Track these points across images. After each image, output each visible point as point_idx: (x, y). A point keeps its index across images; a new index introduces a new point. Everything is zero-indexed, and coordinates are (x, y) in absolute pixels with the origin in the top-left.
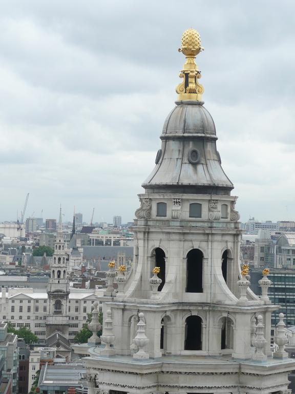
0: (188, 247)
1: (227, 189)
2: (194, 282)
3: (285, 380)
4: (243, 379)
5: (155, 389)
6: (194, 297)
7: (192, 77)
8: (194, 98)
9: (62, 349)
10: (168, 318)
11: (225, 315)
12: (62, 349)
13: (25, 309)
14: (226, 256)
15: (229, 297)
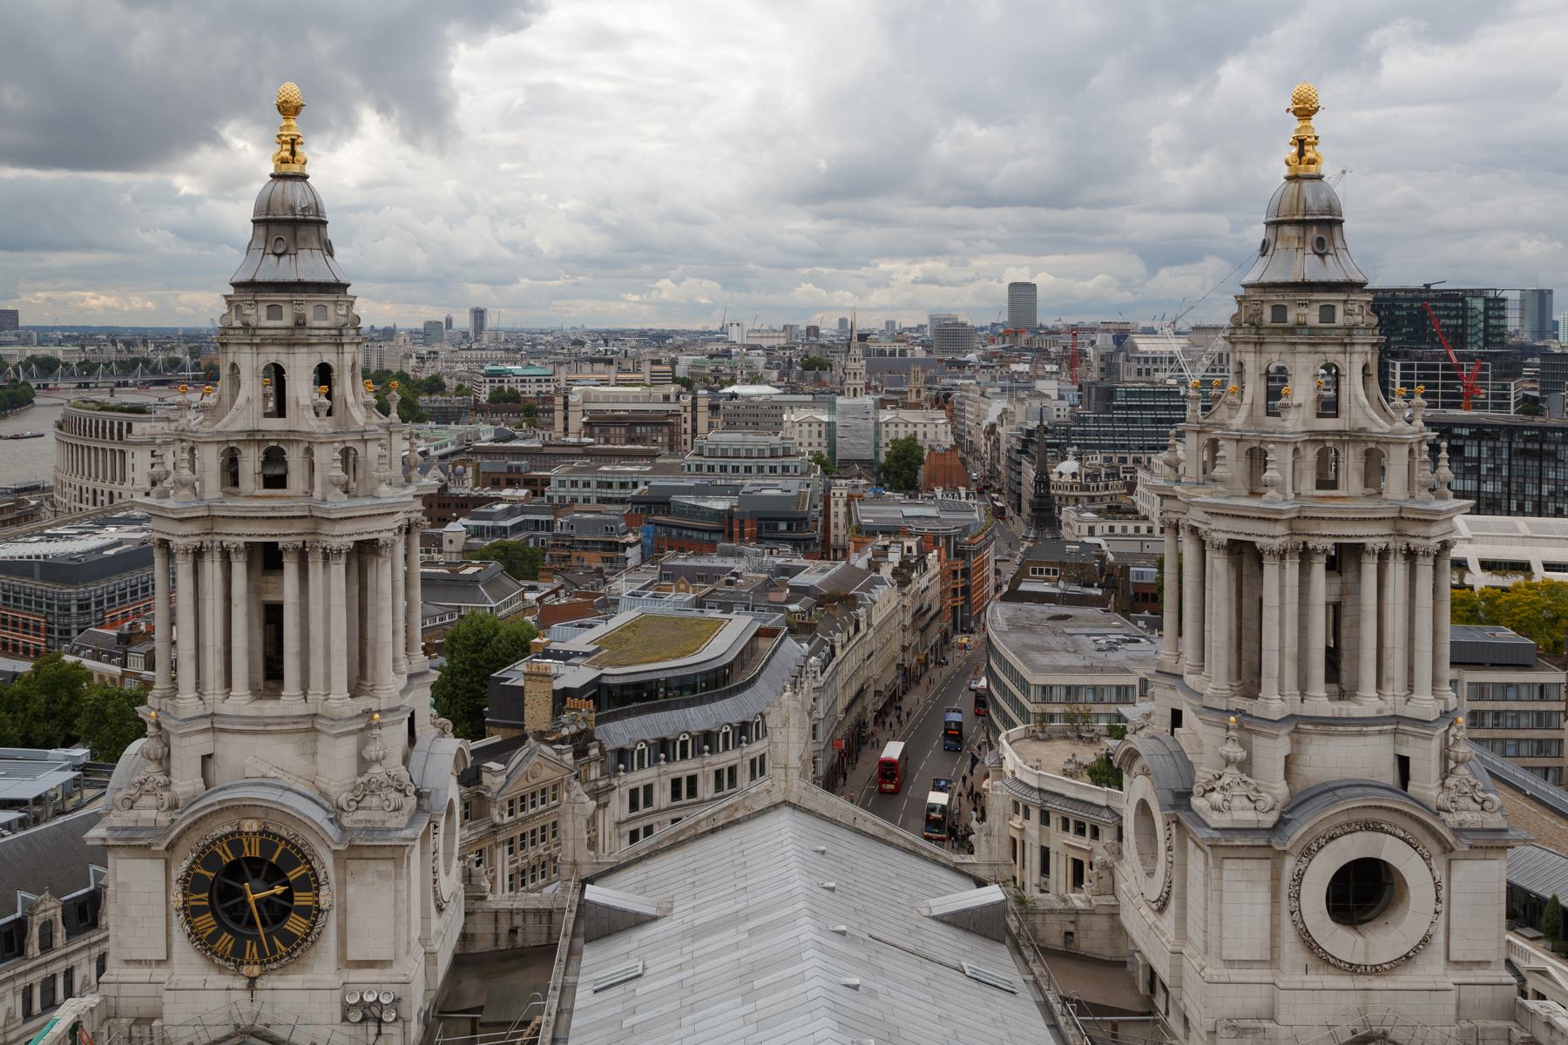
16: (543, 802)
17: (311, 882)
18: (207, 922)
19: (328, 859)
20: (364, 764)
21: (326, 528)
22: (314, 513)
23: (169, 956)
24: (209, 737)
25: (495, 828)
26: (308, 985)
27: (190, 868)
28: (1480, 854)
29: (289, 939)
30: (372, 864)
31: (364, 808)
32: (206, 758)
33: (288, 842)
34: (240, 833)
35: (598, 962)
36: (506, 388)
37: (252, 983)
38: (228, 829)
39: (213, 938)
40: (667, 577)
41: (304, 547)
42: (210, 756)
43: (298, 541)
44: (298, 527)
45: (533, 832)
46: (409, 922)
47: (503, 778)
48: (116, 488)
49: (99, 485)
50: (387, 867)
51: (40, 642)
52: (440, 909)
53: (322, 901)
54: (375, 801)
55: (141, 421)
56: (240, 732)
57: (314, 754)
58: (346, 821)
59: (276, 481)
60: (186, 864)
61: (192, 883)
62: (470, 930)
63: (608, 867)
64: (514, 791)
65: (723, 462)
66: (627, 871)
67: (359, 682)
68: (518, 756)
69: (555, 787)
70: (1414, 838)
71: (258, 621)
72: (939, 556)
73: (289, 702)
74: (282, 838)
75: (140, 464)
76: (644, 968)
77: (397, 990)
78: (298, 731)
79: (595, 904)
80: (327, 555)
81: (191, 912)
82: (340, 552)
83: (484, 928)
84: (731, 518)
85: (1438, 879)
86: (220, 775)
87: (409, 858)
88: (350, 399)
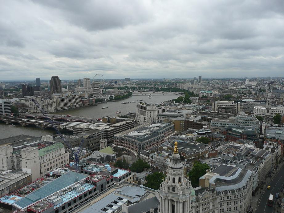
9: (269, 121)
12: (269, 121)
13: (260, 111)
25: (200, 204)
36: (204, 95)
40: (230, 147)
47: (201, 196)
48: (145, 117)
49: (143, 116)
51: (137, 149)
55: (149, 107)
64: (203, 198)
65: (241, 121)
71: (172, 206)
72: (281, 146)
75: (148, 113)
84: (242, 134)
88: (183, 181)
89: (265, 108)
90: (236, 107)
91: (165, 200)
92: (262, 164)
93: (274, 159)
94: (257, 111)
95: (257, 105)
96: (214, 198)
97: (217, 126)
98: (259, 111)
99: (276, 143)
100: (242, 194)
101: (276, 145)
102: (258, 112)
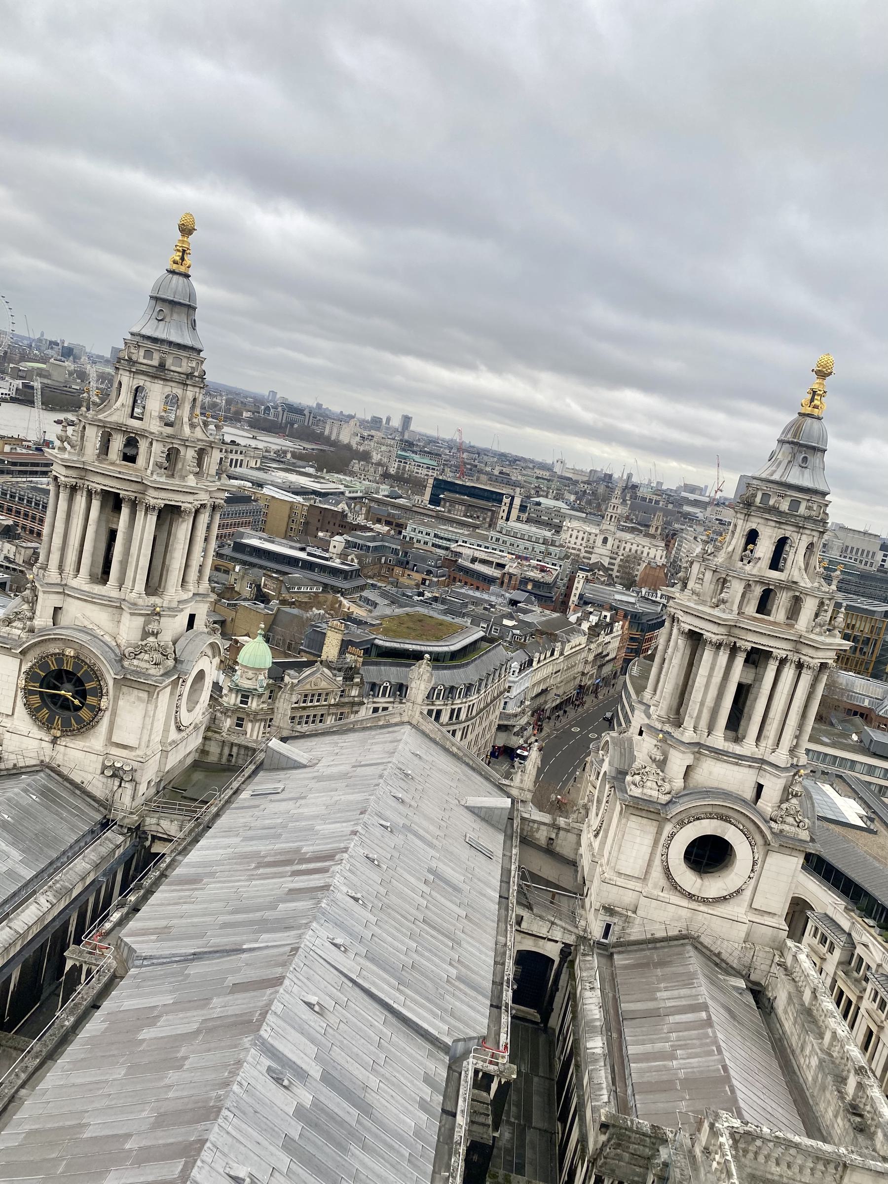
0: (779, 534)
1: (824, 494)
2: (776, 563)
3: (833, 654)
4: (799, 646)
5: (725, 637)
6: (775, 574)
7: (818, 395)
8: (816, 412)
9: (601, 573)
10: (749, 585)
11: (797, 594)
12: (601, 573)
13: (580, 538)
14: (810, 547)
15: (805, 582)
16: (318, 701)
17: (99, 693)
18: (36, 700)
19: (111, 683)
20: (146, 634)
21: (151, 493)
22: (144, 481)
23: (13, 714)
24: (61, 597)
26: (85, 749)
27: (31, 667)
28: (788, 851)
29: (79, 720)
30: (136, 691)
31: (139, 659)
32: (57, 610)
33: (89, 666)
34: (64, 655)
35: (264, 782)
37: (54, 741)
38: (57, 651)
39: (38, 710)
41: (136, 500)
42: (60, 608)
43: (132, 495)
44: (134, 487)
45: (308, 717)
46: (151, 729)
50: (144, 695)
52: (179, 729)
53: (102, 705)
54: (146, 657)
56: (78, 598)
57: (119, 622)
58: (126, 663)
59: (130, 458)
60: (30, 664)
61: (31, 676)
62: (207, 748)
63: (297, 734)
66: (309, 739)
67: (153, 586)
68: (308, 672)
69: (327, 694)
70: (748, 831)
73: (110, 590)
74: (86, 663)
76: (283, 790)
77: (136, 765)
78: (111, 606)
79: (272, 749)
80: (147, 508)
81: (28, 693)
82: (154, 508)
83: (214, 749)
85: (756, 858)
86: (64, 620)
87: (158, 694)
89: (598, 532)
90: (506, 511)
91: (74, 489)
92: (549, 654)
93: (591, 657)
94: (571, 536)
95: (571, 517)
96: (346, 700)
97: (426, 543)
98: (577, 538)
99: (608, 614)
100: (460, 709)
101: (608, 620)
102: (573, 540)
